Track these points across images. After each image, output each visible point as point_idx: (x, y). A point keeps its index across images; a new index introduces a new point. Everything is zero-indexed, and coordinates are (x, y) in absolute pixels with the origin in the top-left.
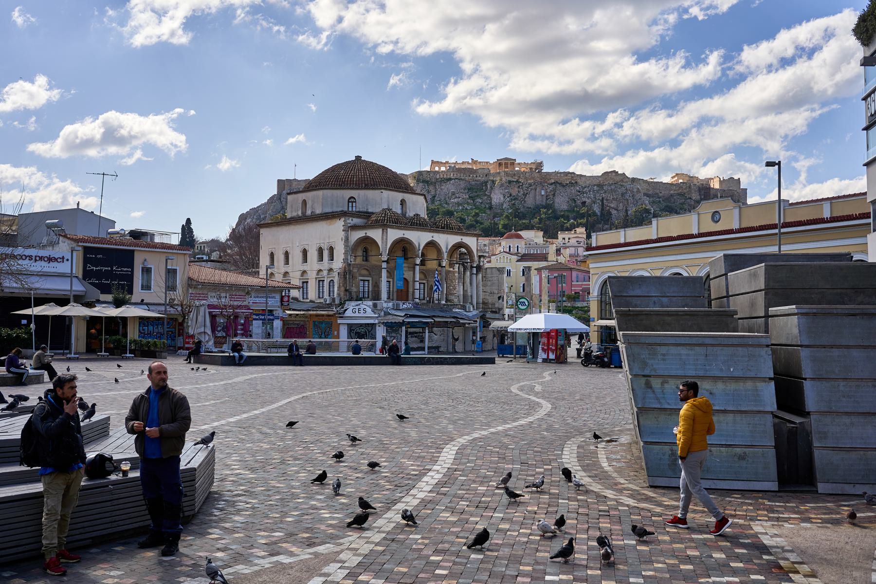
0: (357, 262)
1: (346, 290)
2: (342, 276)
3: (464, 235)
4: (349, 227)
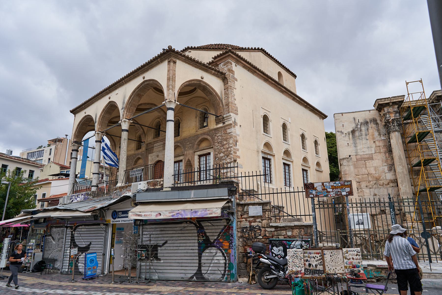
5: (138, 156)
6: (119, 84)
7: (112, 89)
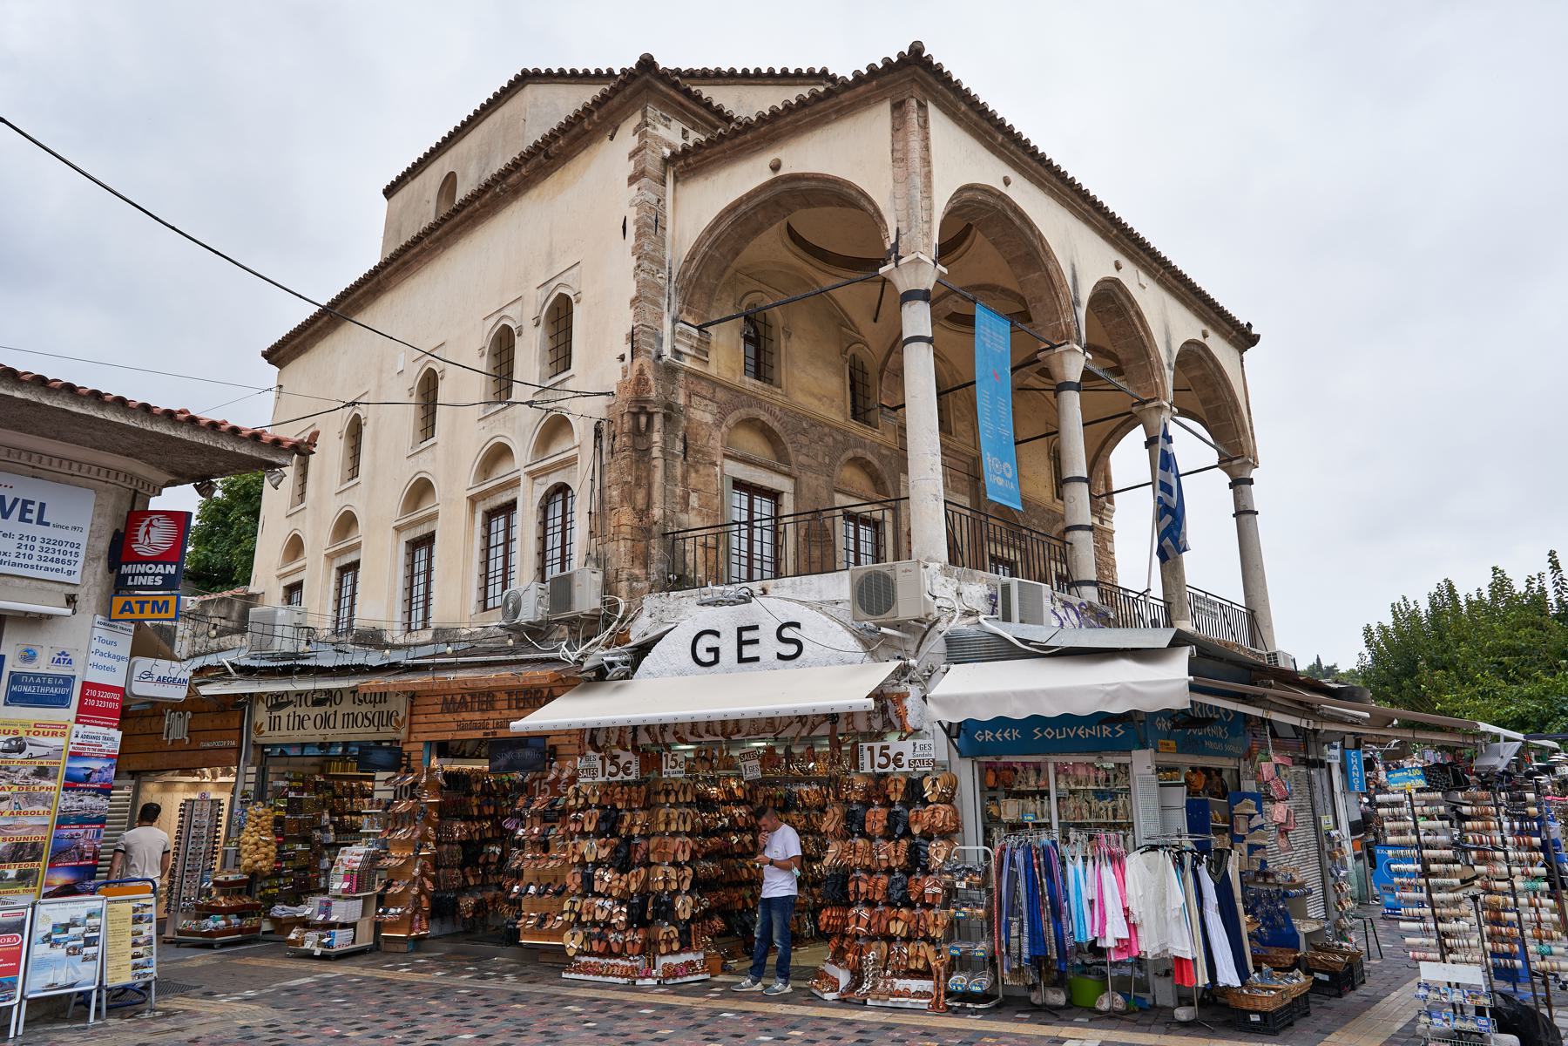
0: (712, 370)
1: (644, 531)
4: (666, 162)
5: (860, 452)
6: (1148, 259)
7: (1126, 245)
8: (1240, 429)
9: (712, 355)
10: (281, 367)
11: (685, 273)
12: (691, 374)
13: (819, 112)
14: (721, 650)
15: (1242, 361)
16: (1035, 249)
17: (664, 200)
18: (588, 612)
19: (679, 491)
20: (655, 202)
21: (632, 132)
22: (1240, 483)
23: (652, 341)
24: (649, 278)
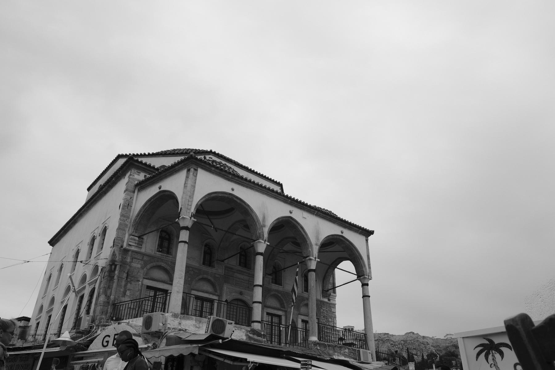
0: (143, 250)
1: (107, 303)
2: (106, 273)
3: (345, 227)
4: (136, 185)
5: (205, 276)
7: (296, 204)
8: (363, 265)
9: (144, 245)
10: (53, 246)
11: (136, 220)
12: (133, 251)
13: (171, 172)
14: (109, 342)
15: (367, 240)
16: (247, 209)
17: (133, 198)
18: (83, 329)
19: (122, 290)
20: (129, 198)
21: (127, 177)
22: (364, 285)
23: (120, 242)
24: (123, 222)
